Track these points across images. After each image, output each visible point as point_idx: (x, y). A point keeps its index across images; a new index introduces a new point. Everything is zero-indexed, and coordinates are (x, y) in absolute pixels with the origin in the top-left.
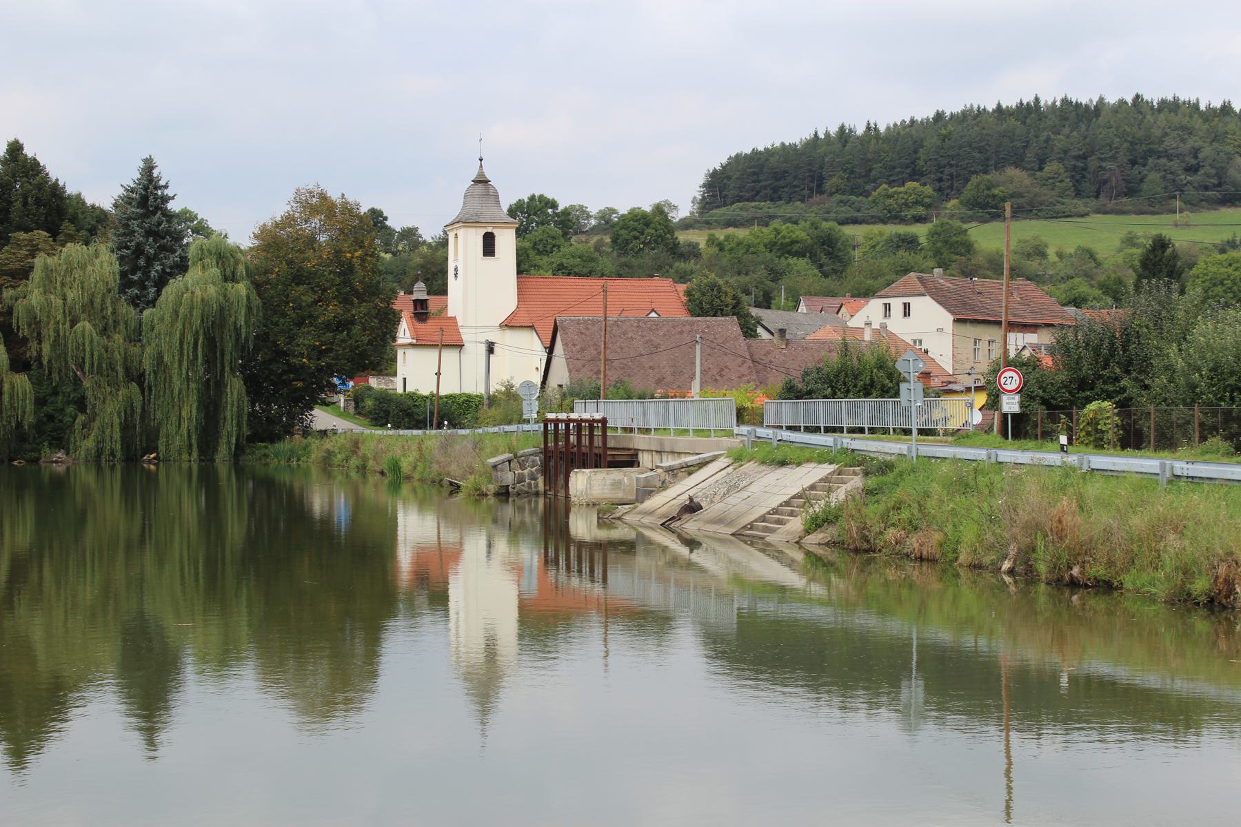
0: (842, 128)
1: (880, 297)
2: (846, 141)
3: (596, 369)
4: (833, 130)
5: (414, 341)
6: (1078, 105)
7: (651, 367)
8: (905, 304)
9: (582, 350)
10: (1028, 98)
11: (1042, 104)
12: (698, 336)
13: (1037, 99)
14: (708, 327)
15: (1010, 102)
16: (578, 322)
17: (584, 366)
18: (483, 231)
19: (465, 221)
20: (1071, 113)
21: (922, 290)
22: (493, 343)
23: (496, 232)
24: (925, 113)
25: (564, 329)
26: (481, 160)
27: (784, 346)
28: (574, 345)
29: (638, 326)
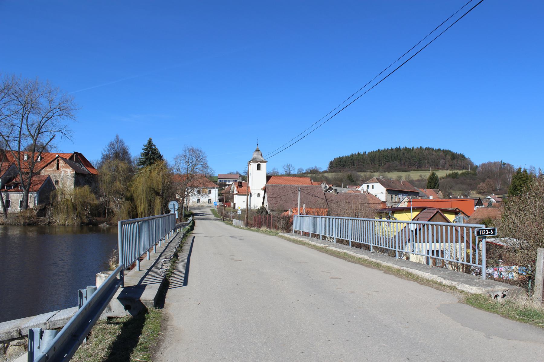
0: (358, 153)
1: (366, 183)
2: (359, 155)
3: (276, 200)
4: (357, 153)
5: (238, 193)
6: (408, 148)
7: (294, 200)
8: (373, 185)
9: (273, 194)
10: (398, 147)
11: (401, 148)
12: (299, 188)
13: (400, 147)
14: (313, 188)
15: (394, 148)
16: (272, 186)
17: (272, 199)
18: (257, 163)
19: (254, 160)
20: (407, 150)
21: (377, 181)
22: (259, 194)
23: (261, 164)
24: (376, 150)
25: (268, 188)
26: (258, 145)
27: (336, 195)
28: (270, 193)
29: (291, 188)
